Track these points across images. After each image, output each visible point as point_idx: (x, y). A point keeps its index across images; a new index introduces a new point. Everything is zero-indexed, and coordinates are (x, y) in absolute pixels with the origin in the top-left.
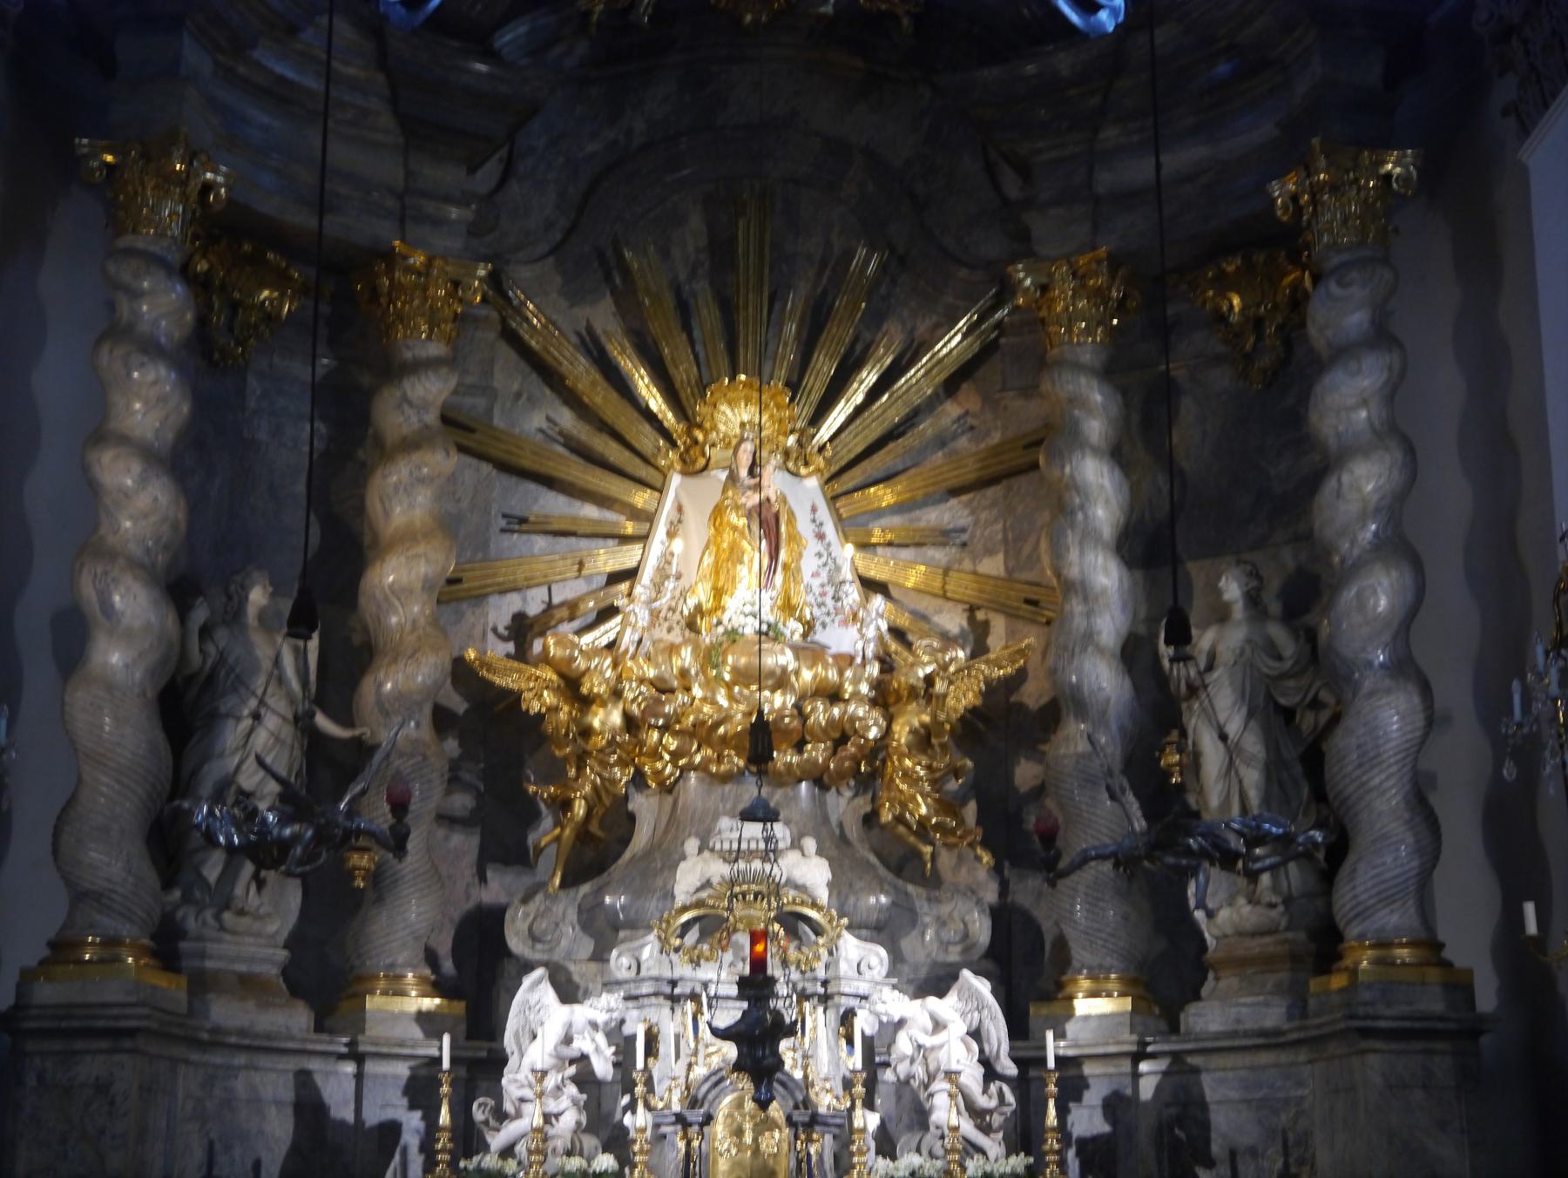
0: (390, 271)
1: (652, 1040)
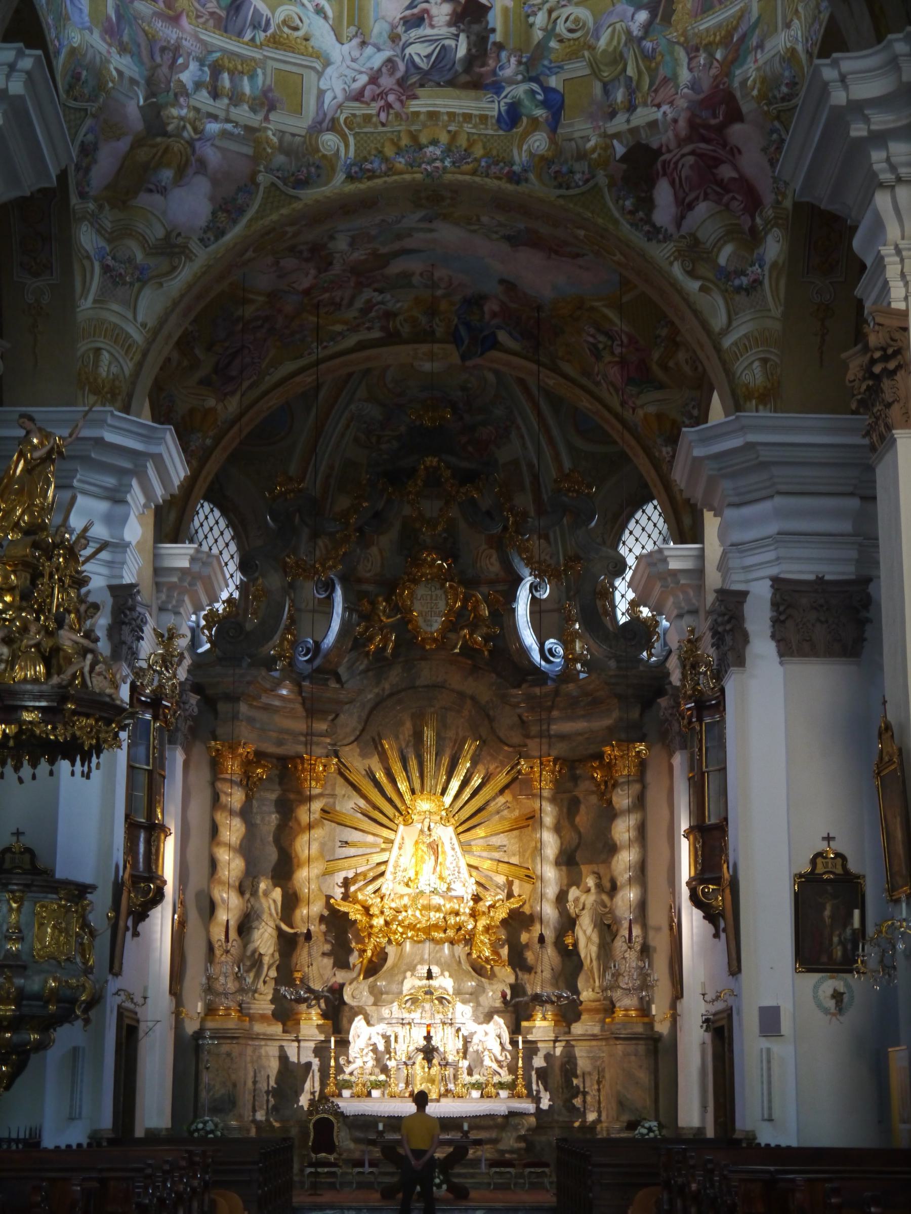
0: (303, 764)
1: (396, 1037)
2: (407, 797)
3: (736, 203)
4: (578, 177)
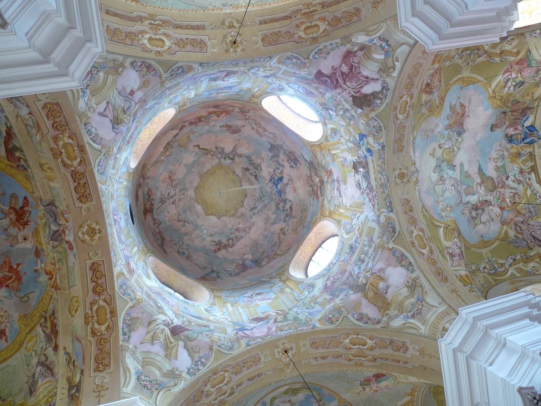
3: (355, 61)
4: (375, 124)
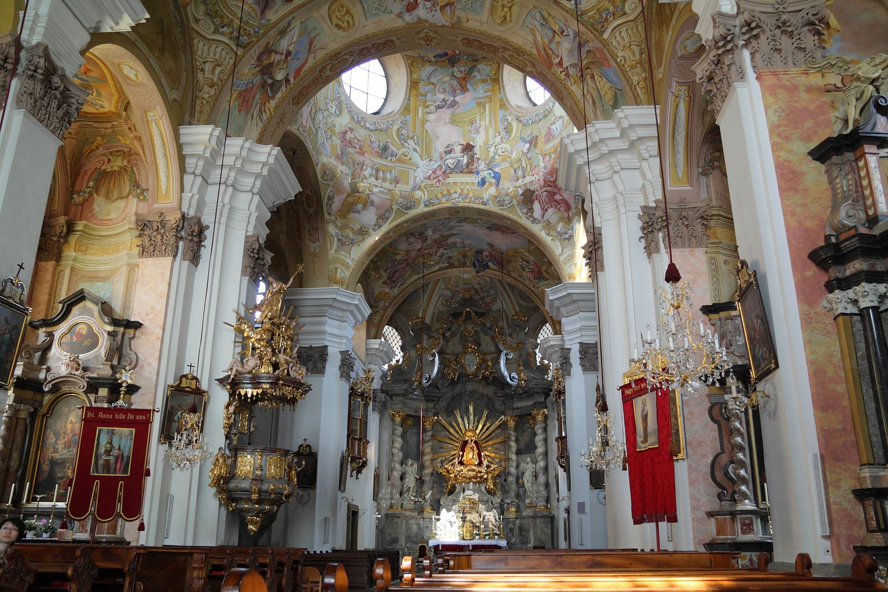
2: (463, 431)
